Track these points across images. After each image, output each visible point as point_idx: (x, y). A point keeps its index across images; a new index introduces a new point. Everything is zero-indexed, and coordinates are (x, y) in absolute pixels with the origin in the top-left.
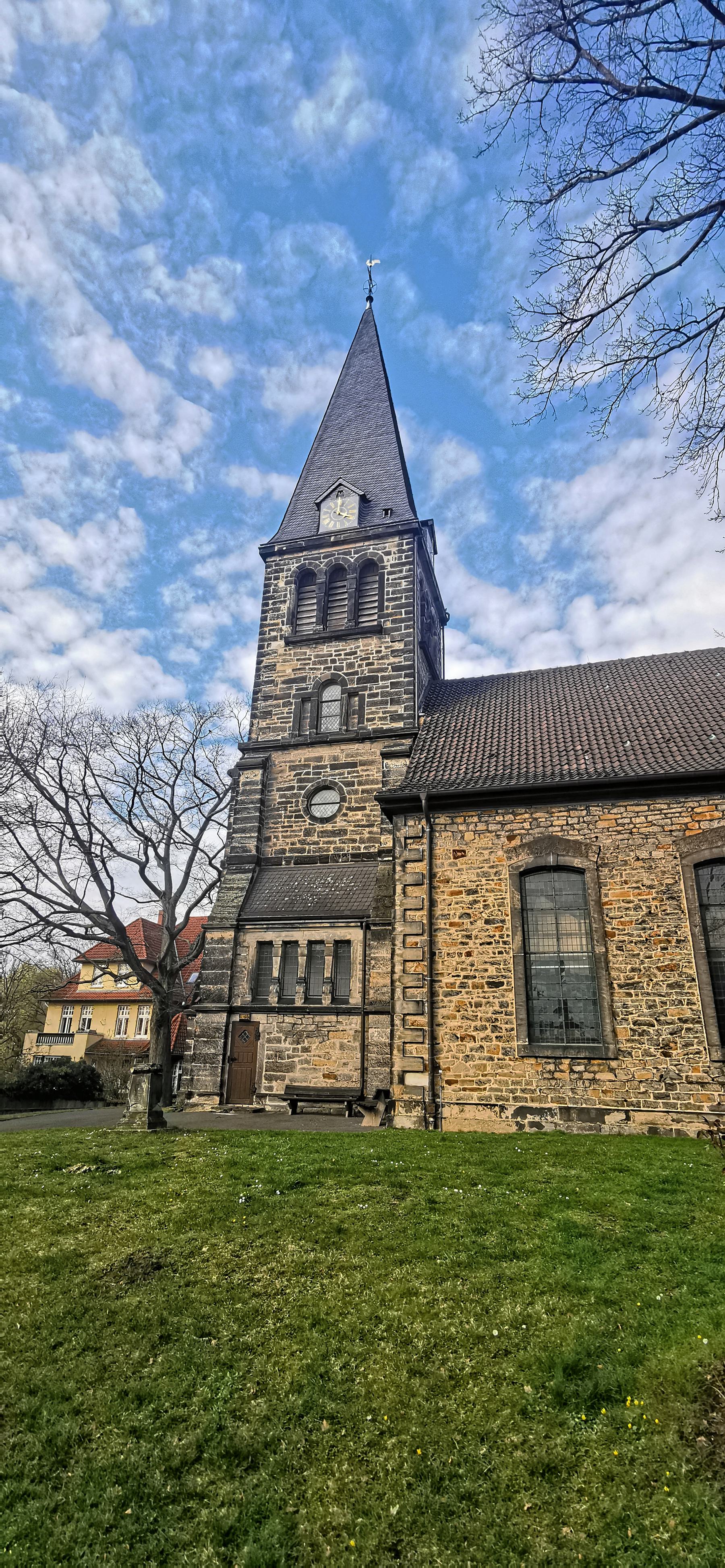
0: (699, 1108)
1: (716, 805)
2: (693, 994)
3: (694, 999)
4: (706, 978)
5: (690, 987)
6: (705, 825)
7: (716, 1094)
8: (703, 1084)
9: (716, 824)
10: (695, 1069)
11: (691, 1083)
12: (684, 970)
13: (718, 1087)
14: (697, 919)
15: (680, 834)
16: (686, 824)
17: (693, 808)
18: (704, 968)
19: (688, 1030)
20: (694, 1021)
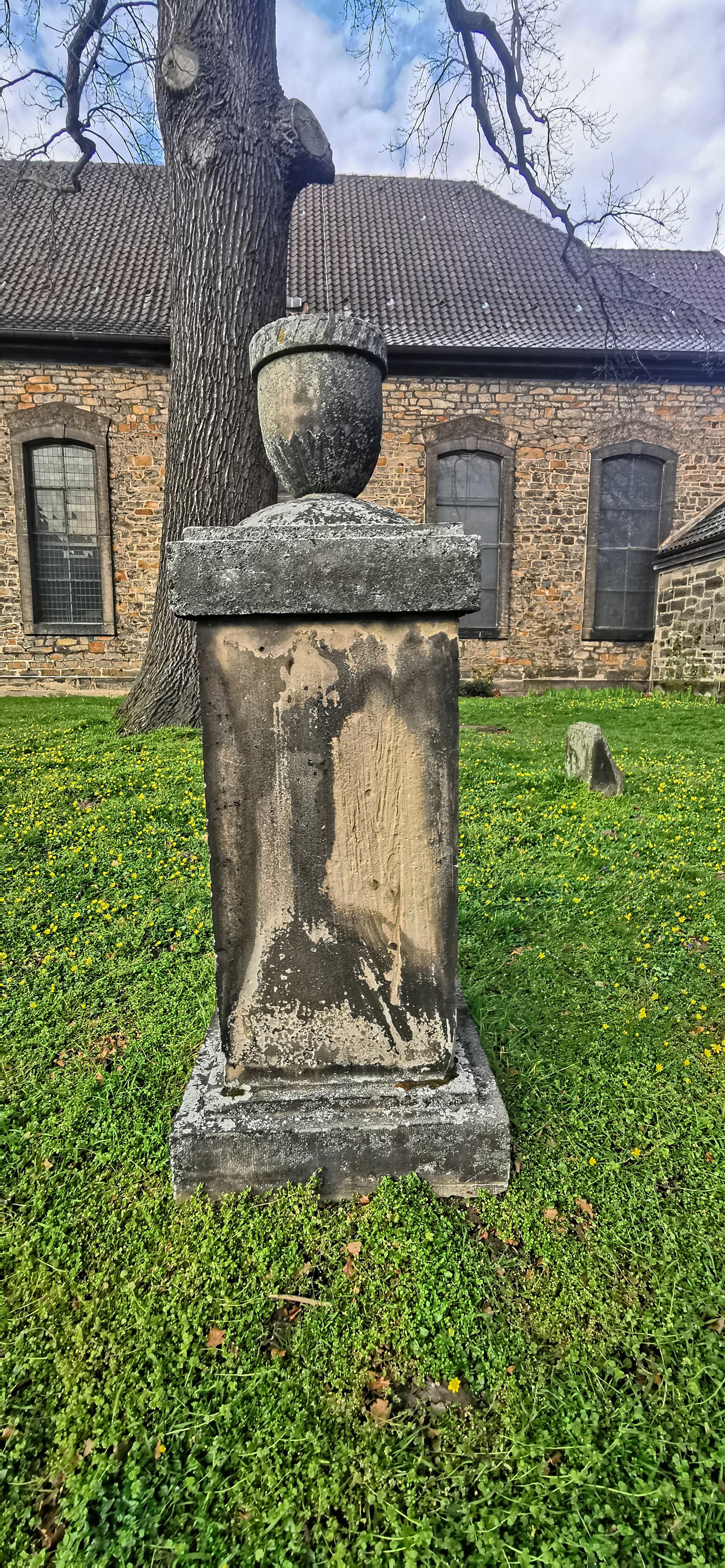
0: (13, 673)
1: (51, 377)
2: (15, 576)
3: (16, 580)
4: (26, 561)
5: (12, 569)
6: (38, 399)
7: (27, 662)
8: (17, 655)
9: (49, 399)
10: (12, 642)
11: (7, 653)
12: (9, 553)
13: (30, 656)
14: (23, 502)
15: (12, 407)
16: (19, 396)
17: (27, 377)
18: (25, 550)
19: (8, 608)
20: (13, 600)
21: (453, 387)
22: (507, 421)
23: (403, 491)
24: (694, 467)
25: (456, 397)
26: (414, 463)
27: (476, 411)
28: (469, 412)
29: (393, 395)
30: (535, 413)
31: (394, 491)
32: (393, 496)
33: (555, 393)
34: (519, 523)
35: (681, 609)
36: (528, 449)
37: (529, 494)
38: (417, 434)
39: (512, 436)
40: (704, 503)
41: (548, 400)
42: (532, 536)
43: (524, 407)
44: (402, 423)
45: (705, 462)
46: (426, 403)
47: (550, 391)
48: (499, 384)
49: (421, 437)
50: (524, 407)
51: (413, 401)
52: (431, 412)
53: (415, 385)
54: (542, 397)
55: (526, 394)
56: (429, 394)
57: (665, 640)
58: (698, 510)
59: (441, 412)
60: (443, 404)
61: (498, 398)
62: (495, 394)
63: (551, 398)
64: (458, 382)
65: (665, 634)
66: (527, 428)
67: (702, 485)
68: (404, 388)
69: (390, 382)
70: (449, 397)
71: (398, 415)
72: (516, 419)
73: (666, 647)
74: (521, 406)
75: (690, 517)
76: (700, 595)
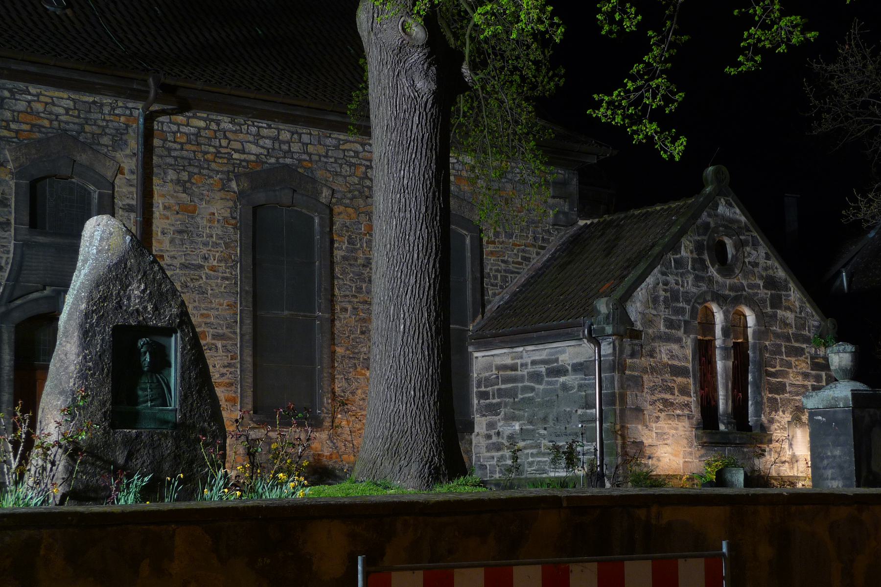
21: (265, 132)
22: (319, 174)
23: (215, 245)
24: (494, 242)
25: (268, 143)
26: (227, 214)
27: (288, 161)
28: (281, 161)
29: (203, 133)
30: (346, 170)
31: (205, 244)
32: (204, 251)
33: (364, 150)
34: (337, 291)
35: (515, 396)
36: (342, 208)
37: (344, 258)
38: (230, 180)
39: (326, 193)
40: (504, 279)
41: (358, 157)
42: (349, 307)
43: (336, 162)
44: (213, 166)
45: (503, 238)
46: (237, 145)
47: (360, 149)
48: (310, 134)
49: (234, 185)
50: (336, 162)
51: (224, 143)
52: (243, 157)
53: (226, 123)
54: (352, 154)
55: (337, 147)
56: (241, 136)
57: (492, 432)
58: (501, 287)
59: (253, 158)
60: (254, 149)
61: (311, 149)
62: (307, 144)
63: (360, 156)
64: (269, 127)
65: (491, 425)
66: (339, 185)
67: (503, 261)
68: (214, 126)
69: (200, 118)
70: (261, 142)
71: (209, 157)
72: (328, 175)
73: (494, 439)
74: (332, 160)
75: (494, 295)
76: (540, 383)
